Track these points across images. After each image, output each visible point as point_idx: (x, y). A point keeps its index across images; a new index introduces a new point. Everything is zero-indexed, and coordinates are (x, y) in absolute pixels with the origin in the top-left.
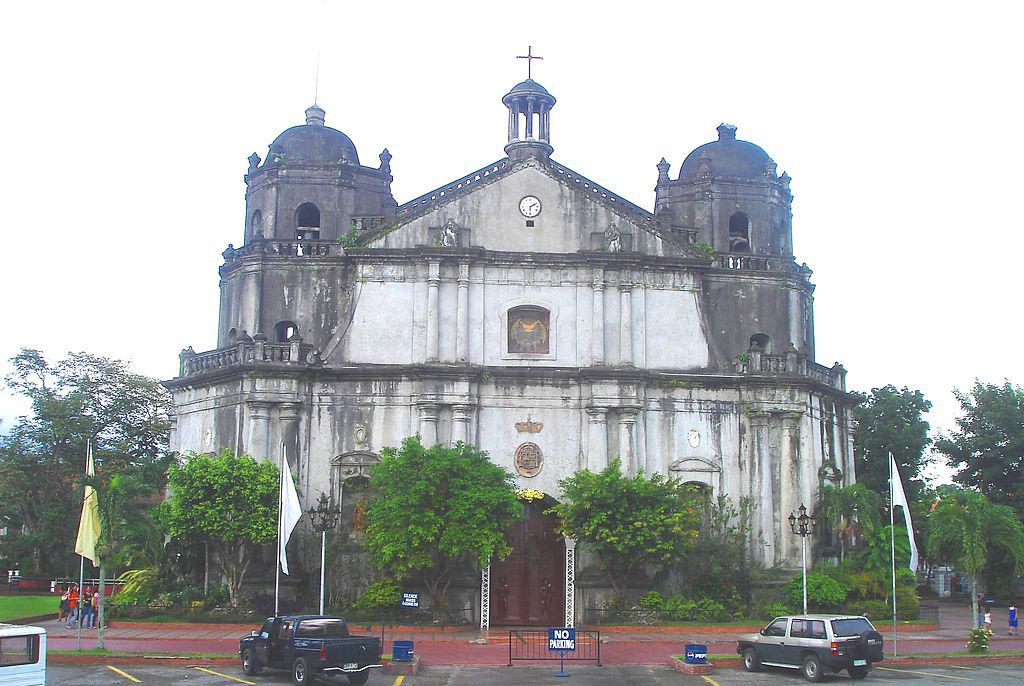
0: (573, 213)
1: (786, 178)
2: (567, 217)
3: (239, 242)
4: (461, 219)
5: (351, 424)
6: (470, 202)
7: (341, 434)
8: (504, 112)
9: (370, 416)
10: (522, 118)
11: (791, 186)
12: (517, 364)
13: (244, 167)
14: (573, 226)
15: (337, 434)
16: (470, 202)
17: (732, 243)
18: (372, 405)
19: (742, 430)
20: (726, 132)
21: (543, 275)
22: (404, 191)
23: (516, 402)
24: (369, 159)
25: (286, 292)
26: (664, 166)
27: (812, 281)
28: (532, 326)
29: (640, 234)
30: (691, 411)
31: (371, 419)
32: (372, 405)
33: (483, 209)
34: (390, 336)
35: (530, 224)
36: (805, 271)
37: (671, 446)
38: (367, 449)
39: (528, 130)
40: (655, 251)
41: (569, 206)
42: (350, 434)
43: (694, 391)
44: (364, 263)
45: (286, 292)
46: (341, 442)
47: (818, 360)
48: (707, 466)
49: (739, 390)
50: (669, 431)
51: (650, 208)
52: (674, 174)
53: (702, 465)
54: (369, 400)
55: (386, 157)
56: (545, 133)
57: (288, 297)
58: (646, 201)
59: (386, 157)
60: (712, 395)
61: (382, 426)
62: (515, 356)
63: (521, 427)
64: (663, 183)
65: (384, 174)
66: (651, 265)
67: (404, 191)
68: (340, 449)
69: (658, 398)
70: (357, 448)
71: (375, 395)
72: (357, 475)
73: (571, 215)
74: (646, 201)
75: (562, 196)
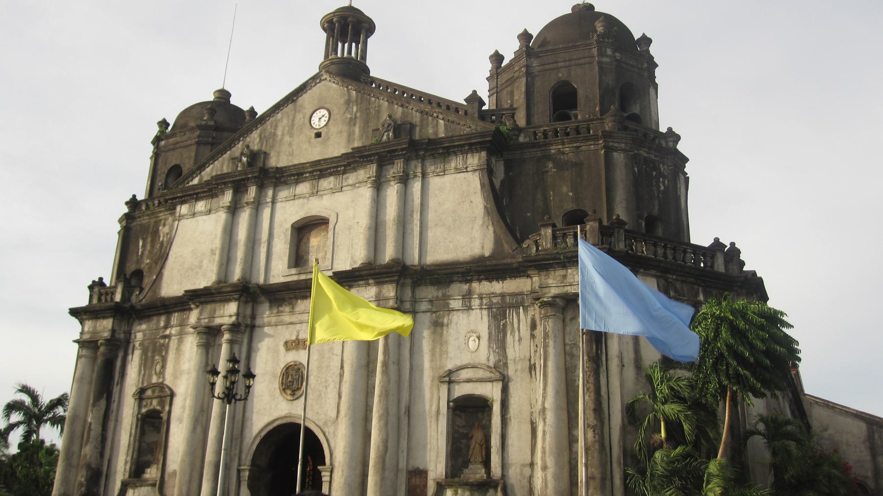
0: (358, 115)
2: (352, 122)
4: (259, 145)
5: (153, 357)
6: (269, 127)
7: (145, 367)
9: (166, 347)
12: (295, 278)
14: (357, 130)
15: (142, 369)
16: (269, 127)
18: (168, 337)
19: (533, 326)
21: (327, 183)
23: (287, 318)
25: (141, 243)
26: (497, 58)
29: (422, 121)
30: (470, 308)
31: (167, 352)
32: (168, 337)
33: (279, 133)
34: (193, 267)
35: (318, 135)
37: (444, 353)
38: (161, 380)
40: (436, 133)
41: (355, 109)
42: (151, 368)
43: (475, 285)
44: (182, 203)
45: (141, 243)
46: (144, 375)
49: (528, 276)
50: (441, 335)
53: (481, 374)
54: (168, 332)
57: (142, 247)
60: (497, 287)
61: (174, 356)
62: (293, 271)
63: (290, 346)
66: (426, 150)
68: (143, 383)
69: (430, 296)
70: (154, 380)
71: (172, 327)
72: (152, 407)
73: (356, 117)
75: (348, 102)
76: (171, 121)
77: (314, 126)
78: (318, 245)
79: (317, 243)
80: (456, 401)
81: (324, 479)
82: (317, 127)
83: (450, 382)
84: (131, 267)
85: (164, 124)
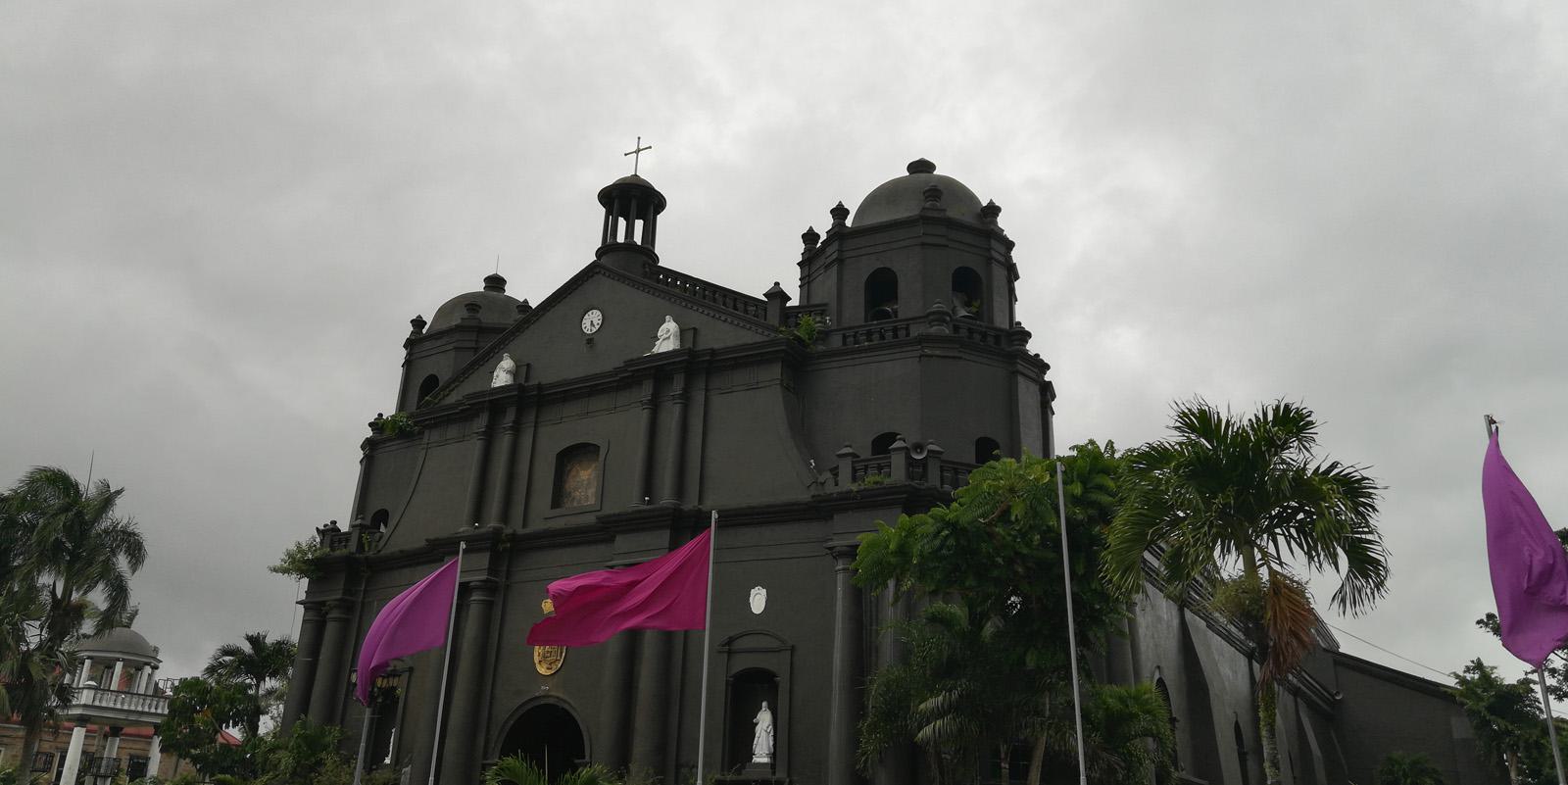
76: (429, 319)
78: (588, 479)
80: (734, 676)
83: (730, 653)
84: (375, 505)
85: (418, 323)
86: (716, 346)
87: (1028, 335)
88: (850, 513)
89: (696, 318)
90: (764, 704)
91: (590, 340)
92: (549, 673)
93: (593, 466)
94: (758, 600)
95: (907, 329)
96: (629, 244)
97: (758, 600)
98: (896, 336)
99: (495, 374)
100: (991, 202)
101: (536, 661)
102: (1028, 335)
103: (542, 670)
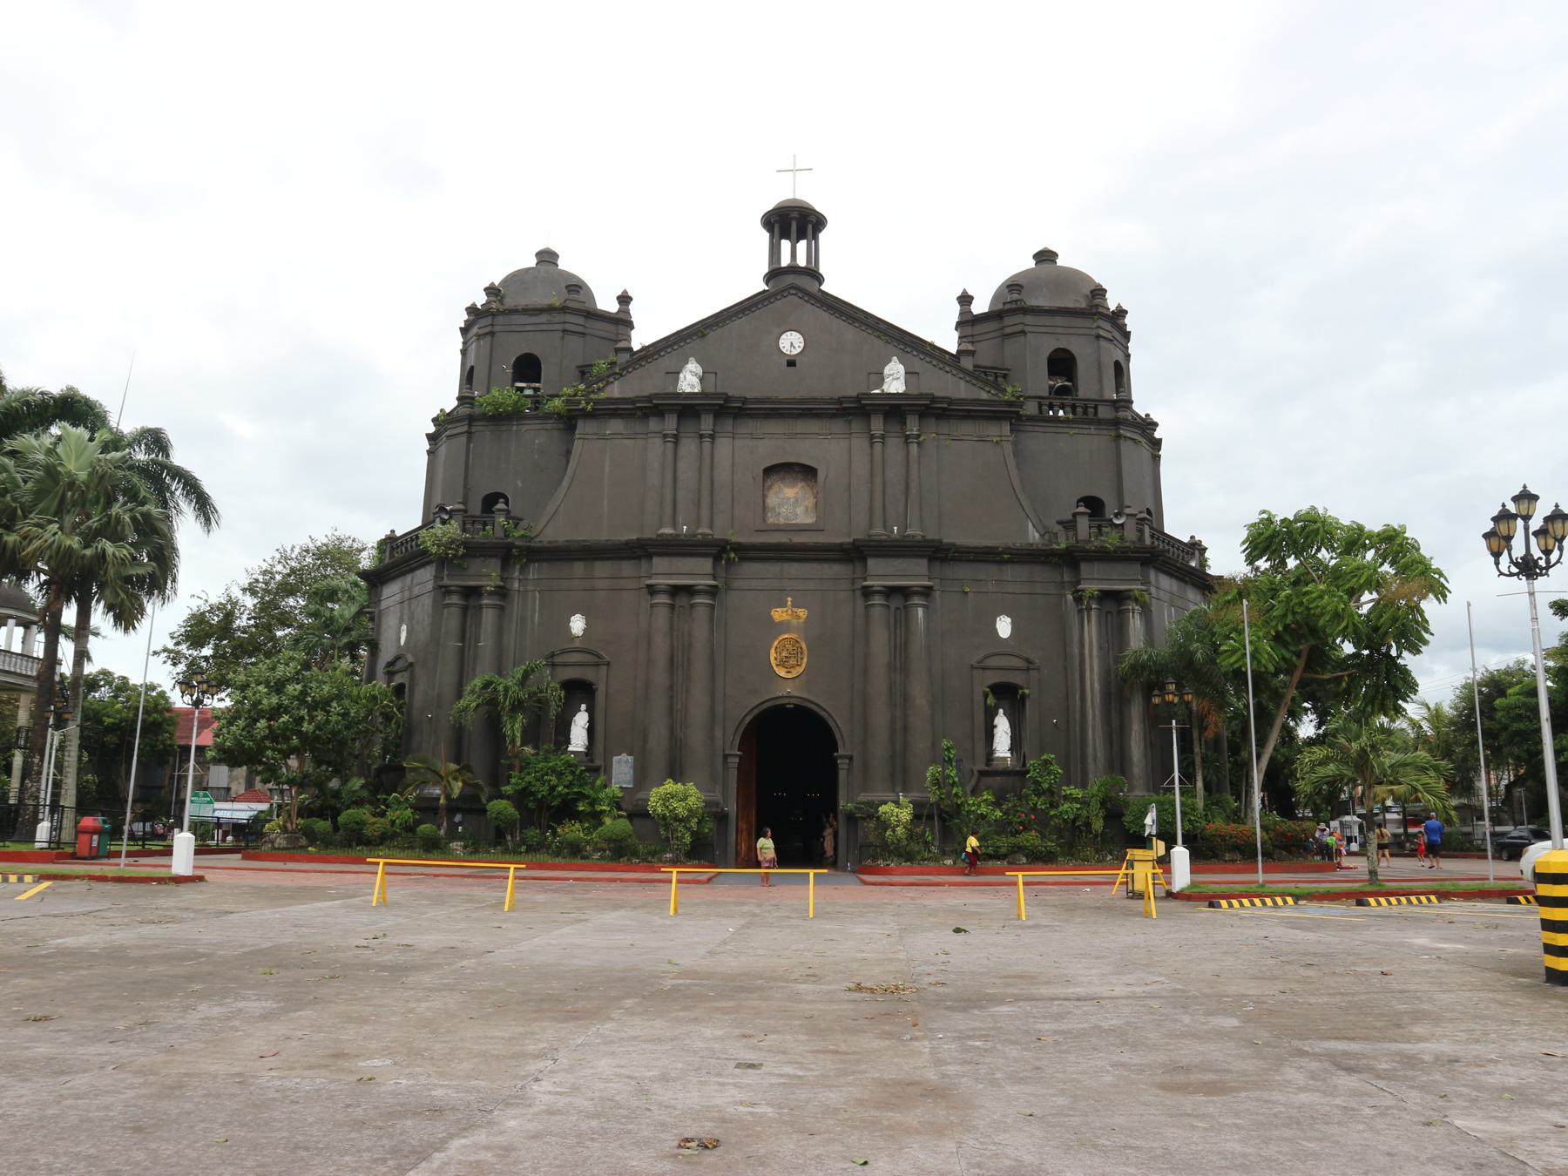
1: (1121, 313)
3: (450, 404)
8: (767, 235)
10: (786, 245)
11: (1127, 321)
13: (462, 318)
17: (1051, 387)
20: (1045, 257)
22: (640, 338)
24: (607, 303)
26: (965, 299)
27: (1157, 435)
28: (795, 490)
36: (1147, 426)
39: (794, 253)
47: (1166, 531)
48: (1022, 664)
51: (953, 348)
52: (980, 307)
55: (624, 299)
56: (813, 254)
58: (949, 341)
59: (624, 299)
64: (967, 322)
65: (622, 322)
67: (640, 338)
74: (949, 341)
77: (784, 351)
79: (793, 495)
81: (840, 766)
82: (788, 353)
86: (937, 394)
87: (1156, 424)
88: (1096, 563)
89: (918, 364)
90: (1001, 711)
91: (791, 363)
92: (790, 676)
93: (800, 485)
94: (1004, 627)
95: (1096, 408)
96: (793, 269)
97: (1004, 627)
98: (1085, 412)
99: (681, 376)
100: (1119, 306)
101: (774, 665)
102: (1156, 424)
103: (782, 672)
